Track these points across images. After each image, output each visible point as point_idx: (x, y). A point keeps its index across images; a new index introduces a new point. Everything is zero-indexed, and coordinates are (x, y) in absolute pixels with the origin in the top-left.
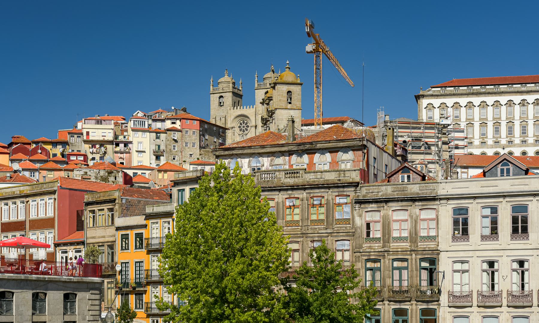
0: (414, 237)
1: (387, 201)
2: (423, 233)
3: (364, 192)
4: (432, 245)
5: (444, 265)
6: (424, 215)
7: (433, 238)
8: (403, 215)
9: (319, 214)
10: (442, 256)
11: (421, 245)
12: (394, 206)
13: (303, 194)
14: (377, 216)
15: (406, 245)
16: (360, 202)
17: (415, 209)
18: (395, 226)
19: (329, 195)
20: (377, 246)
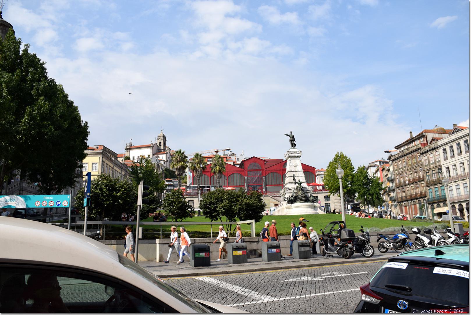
0: (435, 163)
1: (427, 152)
2: (437, 160)
3: (422, 151)
4: (439, 164)
5: (444, 170)
6: (437, 153)
7: (439, 161)
8: (431, 156)
9: (414, 160)
10: (443, 166)
11: (438, 164)
12: (429, 153)
13: (410, 156)
14: (426, 158)
15: (434, 165)
16: (422, 154)
17: (434, 153)
18: (431, 159)
19: (415, 154)
20: (428, 168)
